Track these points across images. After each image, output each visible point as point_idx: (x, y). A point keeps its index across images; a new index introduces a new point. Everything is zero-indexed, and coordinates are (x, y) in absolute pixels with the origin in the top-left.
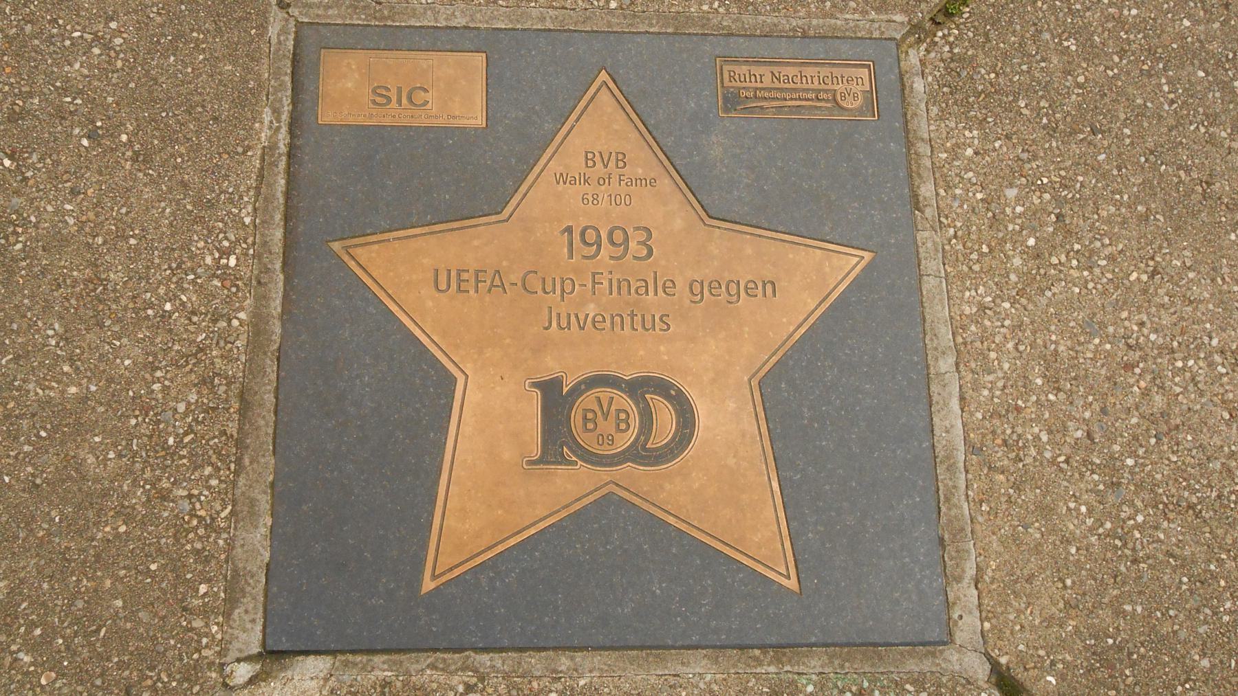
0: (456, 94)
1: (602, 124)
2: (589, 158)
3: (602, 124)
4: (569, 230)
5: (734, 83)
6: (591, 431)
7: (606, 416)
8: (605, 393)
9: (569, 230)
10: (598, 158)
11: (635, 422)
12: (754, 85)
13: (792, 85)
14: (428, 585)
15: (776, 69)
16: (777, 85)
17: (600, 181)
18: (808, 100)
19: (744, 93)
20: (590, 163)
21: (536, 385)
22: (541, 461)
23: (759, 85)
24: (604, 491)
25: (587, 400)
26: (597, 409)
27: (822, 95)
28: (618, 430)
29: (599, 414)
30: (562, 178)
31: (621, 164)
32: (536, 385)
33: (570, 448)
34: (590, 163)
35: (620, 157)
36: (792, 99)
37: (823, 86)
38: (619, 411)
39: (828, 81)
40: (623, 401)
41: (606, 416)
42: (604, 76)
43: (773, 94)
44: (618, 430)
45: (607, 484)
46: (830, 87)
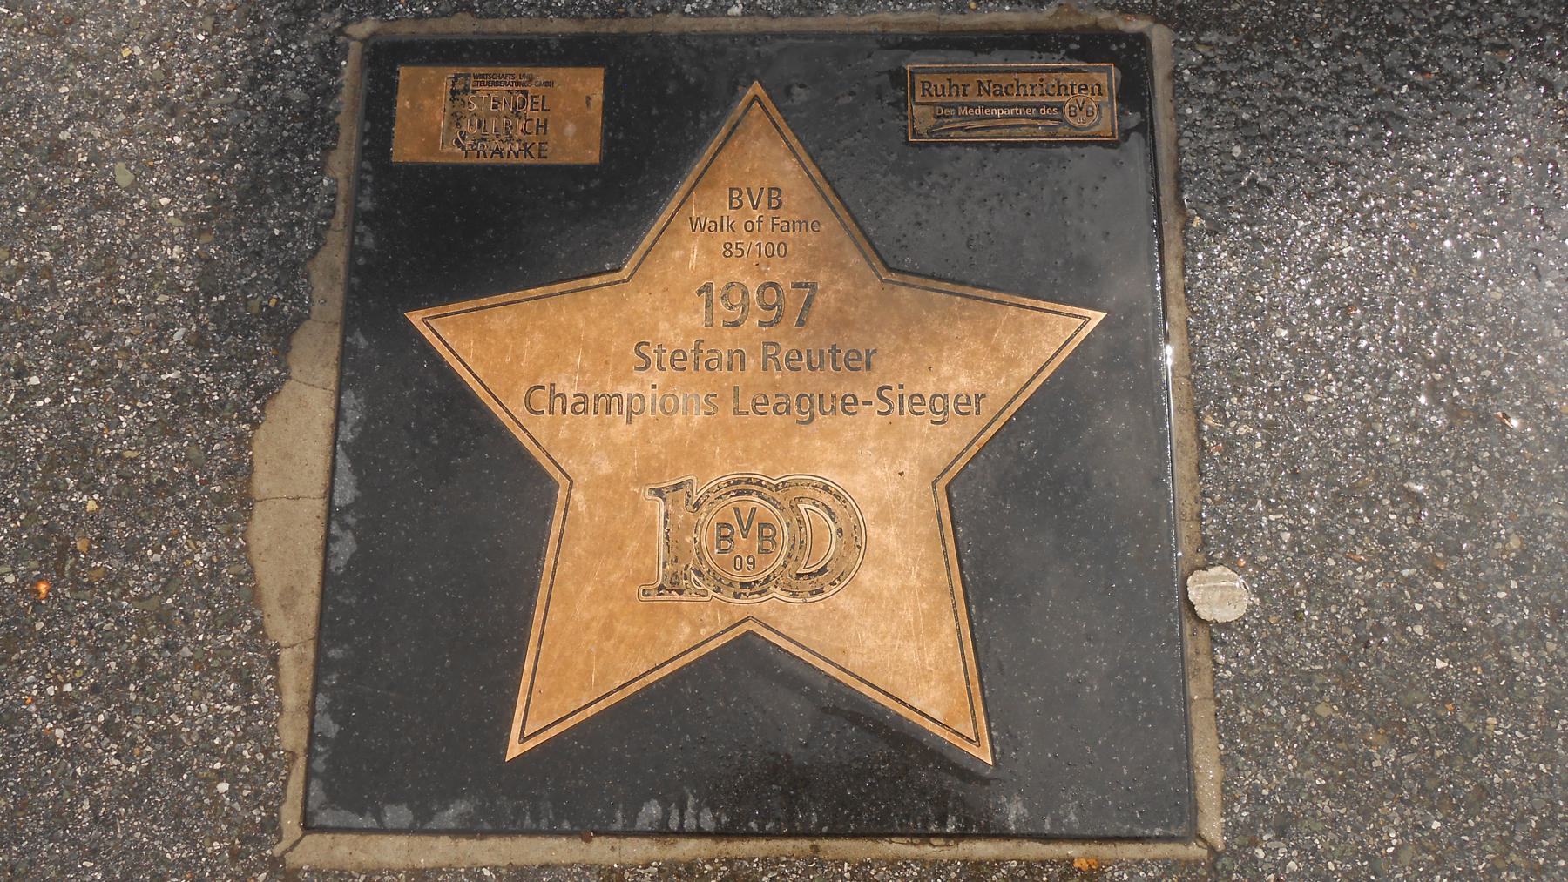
0: (569, 117)
4: (708, 288)
9: (708, 288)
12: (953, 99)
13: (1005, 99)
16: (984, 99)
18: (1027, 117)
20: (736, 203)
23: (961, 99)
26: (734, 522)
27: (1044, 112)
29: (737, 528)
31: (775, 204)
34: (736, 203)
37: (1048, 99)
38: (762, 525)
41: (745, 531)
43: (980, 112)
46: (1056, 99)
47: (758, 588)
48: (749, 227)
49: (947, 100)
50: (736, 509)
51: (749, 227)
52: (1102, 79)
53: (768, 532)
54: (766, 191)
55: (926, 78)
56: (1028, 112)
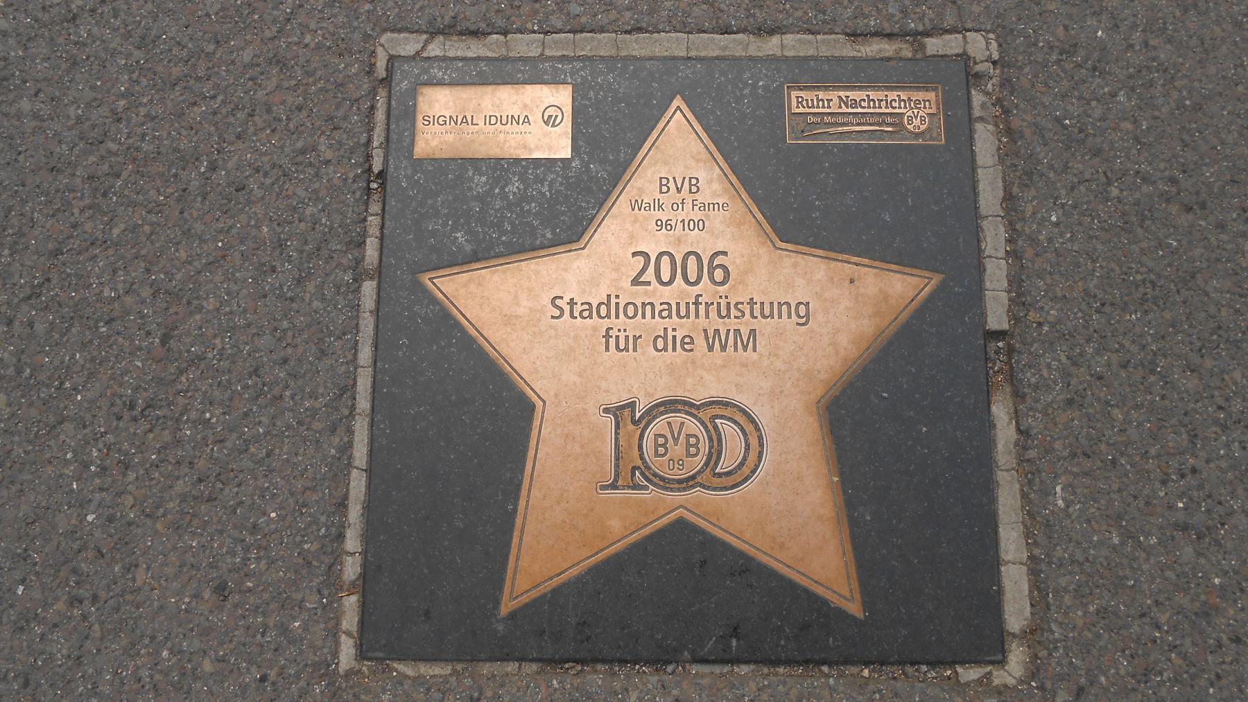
1: (679, 148)
2: (663, 183)
3: (679, 148)
5: (801, 110)
6: (663, 455)
7: (676, 440)
8: (677, 418)
10: (671, 185)
11: (704, 447)
13: (860, 110)
14: (506, 607)
15: (842, 94)
17: (674, 207)
19: (811, 119)
20: (664, 189)
21: (606, 411)
22: (614, 486)
24: (672, 516)
25: (659, 425)
27: (889, 120)
28: (689, 455)
30: (636, 205)
31: (694, 189)
32: (606, 411)
33: (642, 474)
34: (664, 189)
35: (694, 182)
36: (858, 124)
37: (890, 110)
38: (689, 436)
39: (895, 104)
40: (692, 426)
41: (676, 440)
42: (678, 101)
44: (689, 455)
45: (677, 508)
46: (897, 111)
47: (688, 483)
48: (675, 207)
49: (816, 110)
50: (669, 423)
51: (675, 207)
52: (931, 95)
53: (693, 441)
54: (687, 180)
55: (801, 94)
56: (876, 119)
